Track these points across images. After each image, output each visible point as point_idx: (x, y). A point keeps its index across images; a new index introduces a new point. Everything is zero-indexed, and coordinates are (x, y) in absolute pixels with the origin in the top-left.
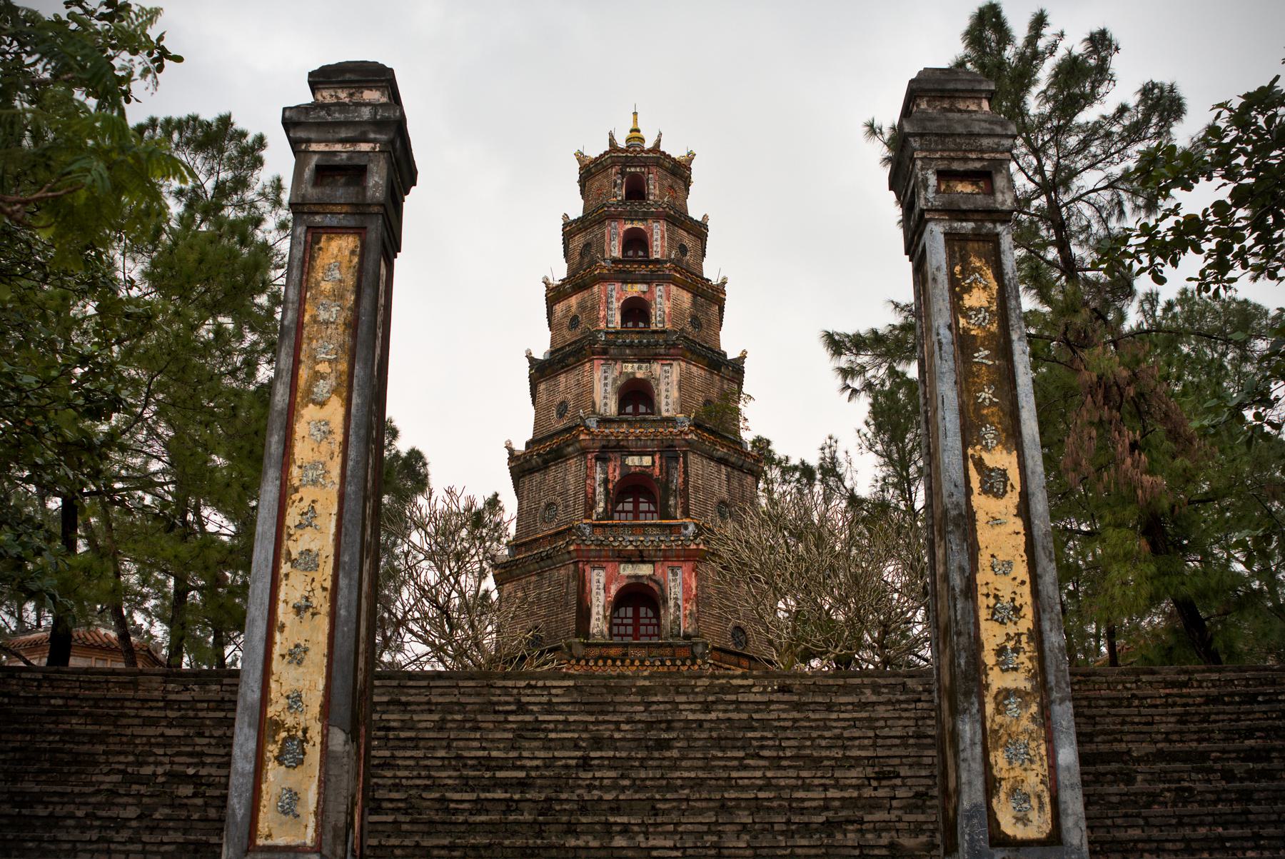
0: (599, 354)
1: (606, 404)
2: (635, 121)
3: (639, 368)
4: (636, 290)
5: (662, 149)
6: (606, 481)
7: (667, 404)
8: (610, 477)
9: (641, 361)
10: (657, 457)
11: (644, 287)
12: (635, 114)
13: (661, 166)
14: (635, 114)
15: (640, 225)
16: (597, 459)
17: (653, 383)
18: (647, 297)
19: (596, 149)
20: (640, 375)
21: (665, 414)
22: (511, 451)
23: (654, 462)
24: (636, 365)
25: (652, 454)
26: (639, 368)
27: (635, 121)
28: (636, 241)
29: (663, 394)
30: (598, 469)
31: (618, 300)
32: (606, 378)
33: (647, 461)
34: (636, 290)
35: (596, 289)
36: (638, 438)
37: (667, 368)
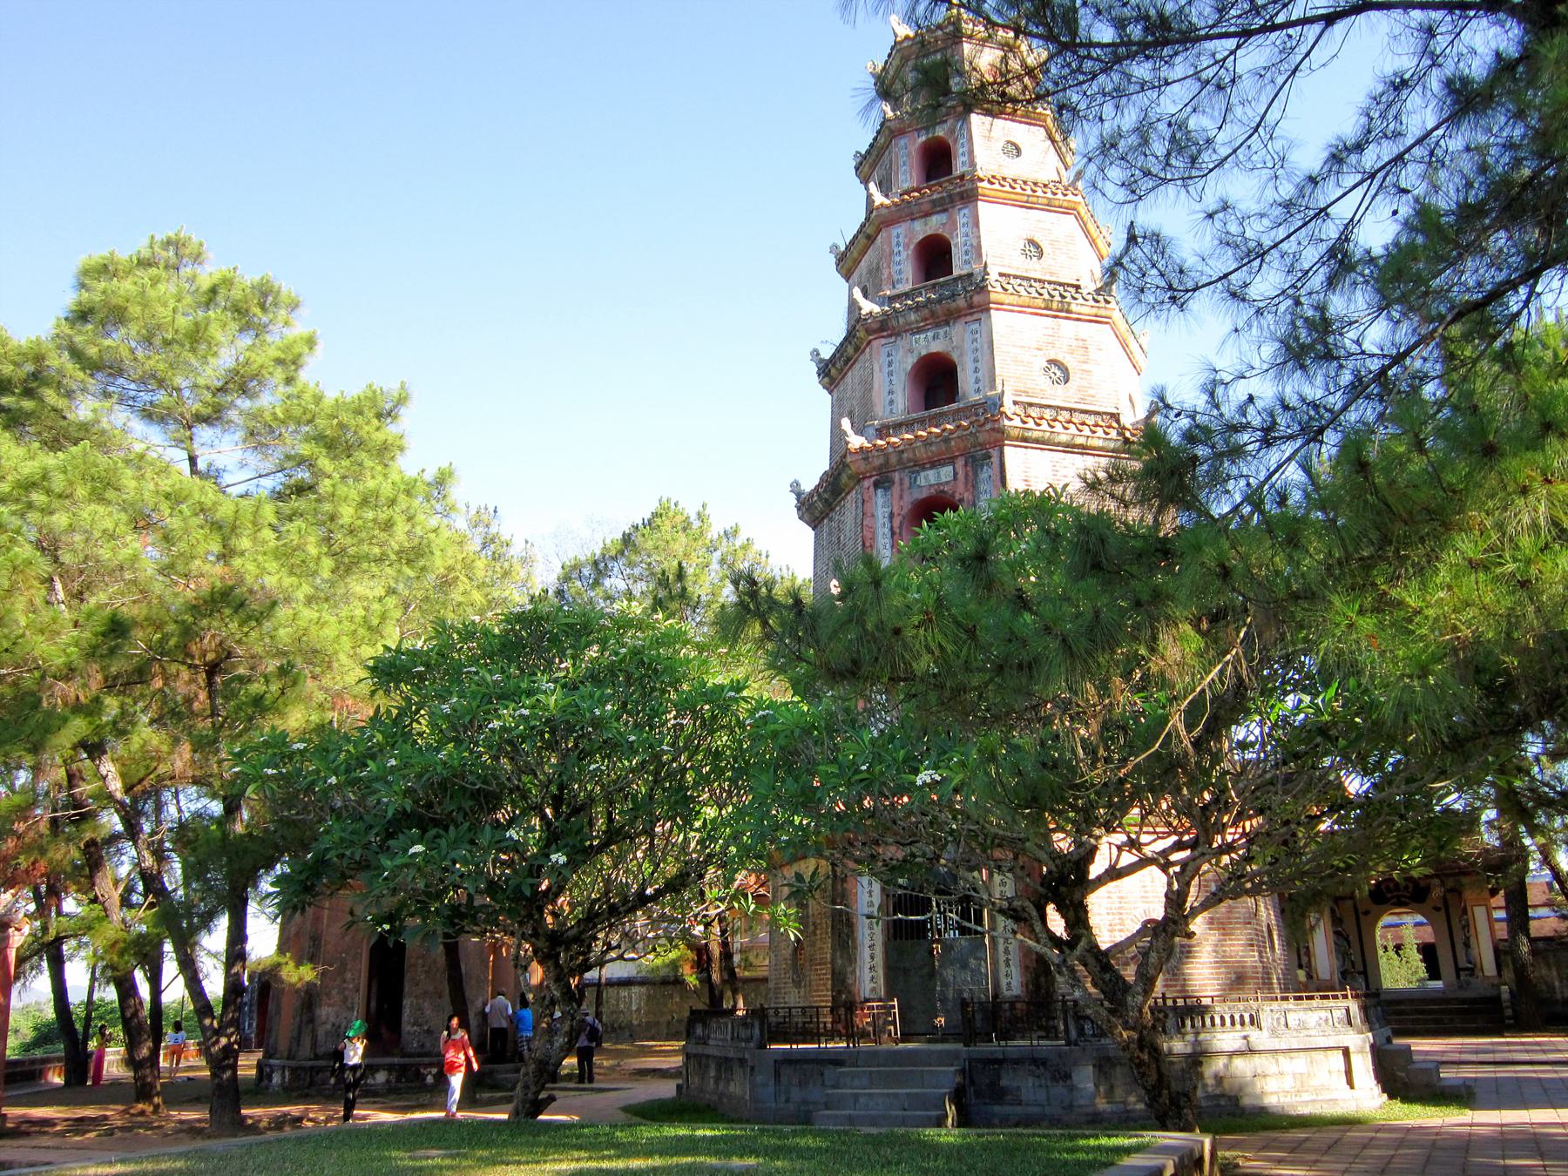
0: (875, 331)
1: (891, 402)
6: (891, 516)
7: (977, 381)
8: (896, 511)
9: (938, 325)
10: (960, 463)
11: (943, 218)
16: (876, 485)
17: (955, 357)
20: (936, 347)
21: (975, 398)
22: (799, 495)
23: (955, 474)
24: (930, 334)
25: (951, 461)
29: (970, 366)
30: (880, 501)
31: (906, 246)
32: (890, 364)
33: (946, 473)
36: (927, 443)
37: (975, 326)
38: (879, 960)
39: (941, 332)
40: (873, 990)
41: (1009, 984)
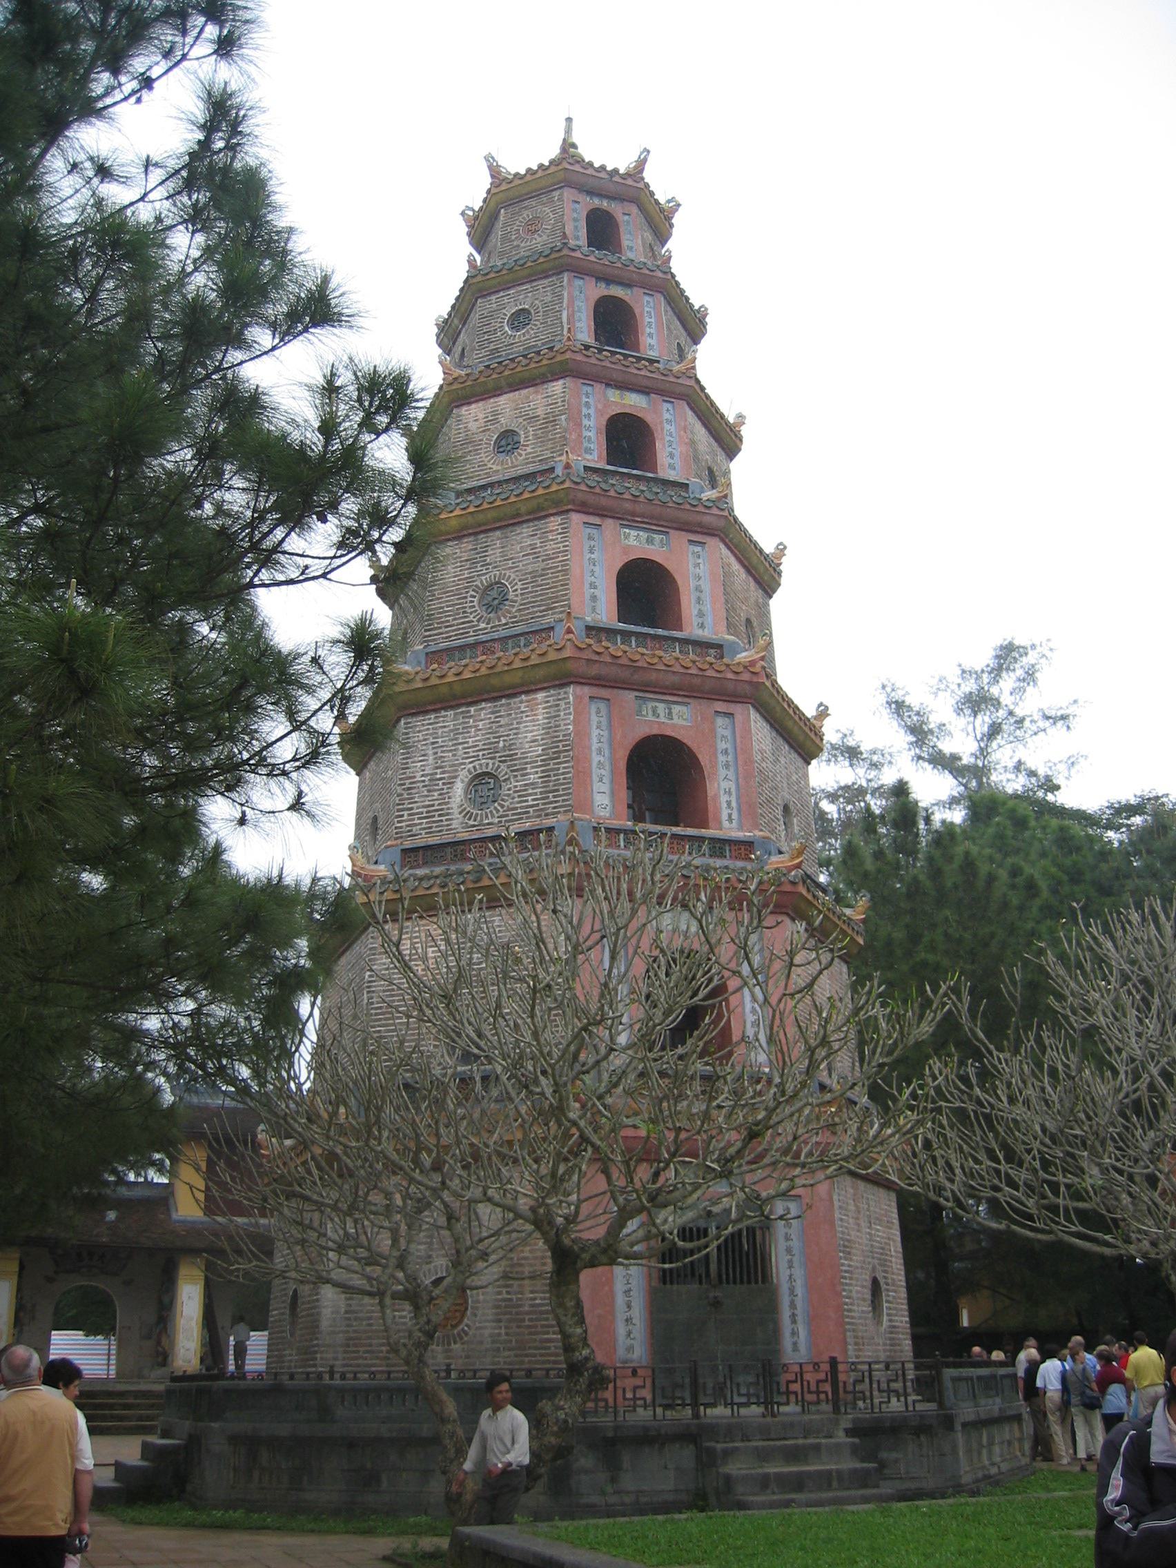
2: (568, 131)
3: (650, 541)
4: (633, 402)
5: (648, 175)
7: (701, 614)
12: (569, 120)
13: (641, 208)
14: (569, 120)
15: (617, 291)
18: (649, 418)
19: (528, 153)
26: (650, 541)
27: (568, 131)
28: (614, 323)
31: (599, 412)
34: (633, 402)
35: (557, 387)
38: (638, 1312)
39: (657, 537)
40: (630, 1349)
41: (795, 1344)
